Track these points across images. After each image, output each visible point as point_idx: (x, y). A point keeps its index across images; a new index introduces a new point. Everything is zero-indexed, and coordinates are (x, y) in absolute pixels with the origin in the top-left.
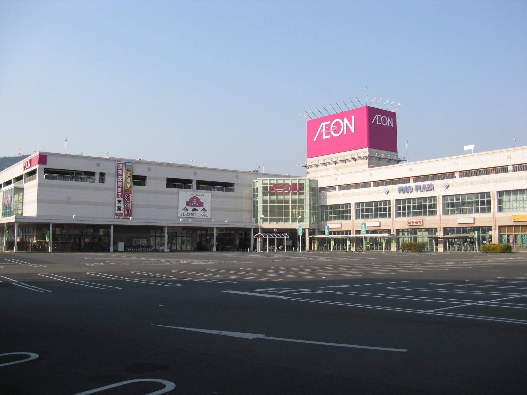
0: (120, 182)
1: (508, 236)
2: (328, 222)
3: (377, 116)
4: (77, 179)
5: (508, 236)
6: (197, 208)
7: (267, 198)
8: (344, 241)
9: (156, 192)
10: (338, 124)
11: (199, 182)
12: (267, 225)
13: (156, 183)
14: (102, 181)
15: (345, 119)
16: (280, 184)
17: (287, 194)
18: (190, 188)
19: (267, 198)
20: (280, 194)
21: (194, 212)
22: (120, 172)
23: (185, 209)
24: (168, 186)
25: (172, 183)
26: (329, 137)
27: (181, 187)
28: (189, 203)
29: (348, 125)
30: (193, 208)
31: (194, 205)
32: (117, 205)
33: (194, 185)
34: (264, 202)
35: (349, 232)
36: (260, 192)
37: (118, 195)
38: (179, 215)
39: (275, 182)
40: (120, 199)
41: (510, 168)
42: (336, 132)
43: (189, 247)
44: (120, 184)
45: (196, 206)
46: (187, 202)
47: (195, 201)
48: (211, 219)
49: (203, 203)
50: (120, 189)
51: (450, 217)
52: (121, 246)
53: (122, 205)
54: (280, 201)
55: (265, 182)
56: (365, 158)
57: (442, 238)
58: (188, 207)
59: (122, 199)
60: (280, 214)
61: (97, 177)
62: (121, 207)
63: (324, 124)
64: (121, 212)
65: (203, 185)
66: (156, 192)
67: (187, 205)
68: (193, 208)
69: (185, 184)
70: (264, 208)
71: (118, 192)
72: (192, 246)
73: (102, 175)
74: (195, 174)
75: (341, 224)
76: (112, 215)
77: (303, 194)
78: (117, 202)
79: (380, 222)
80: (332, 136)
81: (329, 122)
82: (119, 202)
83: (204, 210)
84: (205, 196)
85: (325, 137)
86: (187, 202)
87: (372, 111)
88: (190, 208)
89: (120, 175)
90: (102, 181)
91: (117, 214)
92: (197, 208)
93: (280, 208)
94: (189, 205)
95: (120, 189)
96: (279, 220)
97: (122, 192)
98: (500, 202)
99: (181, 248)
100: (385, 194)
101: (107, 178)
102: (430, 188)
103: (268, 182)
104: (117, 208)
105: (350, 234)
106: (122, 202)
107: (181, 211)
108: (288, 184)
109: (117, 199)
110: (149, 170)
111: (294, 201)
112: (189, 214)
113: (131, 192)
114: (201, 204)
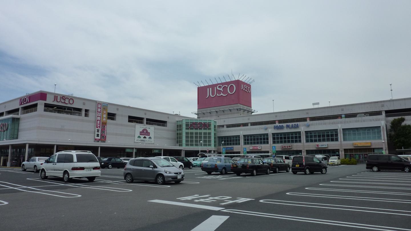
0: (99, 116)
4: (67, 113)
9: (122, 125)
11: (147, 120)
13: (122, 119)
14: (86, 115)
18: (142, 123)
19: (190, 131)
22: (99, 110)
23: (139, 137)
24: (129, 121)
25: (132, 119)
28: (142, 133)
30: (144, 136)
32: (96, 133)
34: (187, 133)
36: (184, 126)
37: (97, 126)
38: (136, 141)
40: (99, 129)
41: (343, 116)
44: (99, 118)
46: (140, 132)
47: (145, 132)
48: (154, 143)
49: (149, 133)
50: (99, 122)
53: (100, 133)
54: (196, 133)
58: (141, 136)
59: (100, 129)
61: (83, 113)
62: (99, 134)
64: (99, 138)
65: (150, 122)
66: (122, 125)
67: (140, 134)
68: (144, 136)
70: (187, 137)
71: (97, 124)
73: (87, 111)
76: (93, 140)
77: (210, 129)
82: (98, 131)
83: (150, 138)
84: (151, 129)
86: (140, 132)
88: (142, 136)
89: (99, 112)
90: (86, 115)
91: (96, 139)
95: (99, 122)
97: (100, 124)
101: (91, 114)
104: (96, 135)
106: (100, 131)
107: (136, 138)
108: (201, 123)
109: (96, 129)
111: (205, 133)
113: (106, 124)
114: (148, 134)
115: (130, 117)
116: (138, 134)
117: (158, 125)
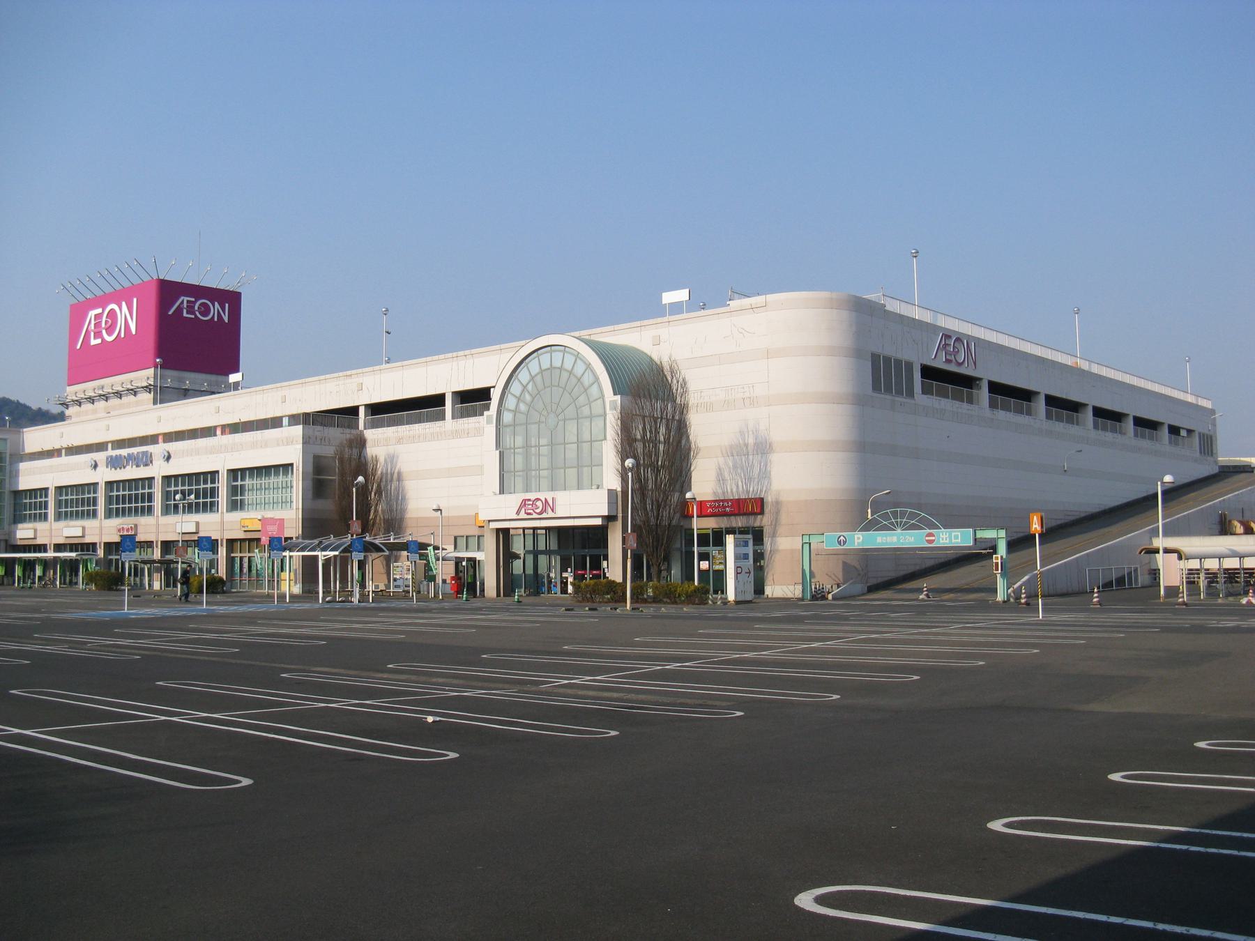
1: (241, 558)
2: (20, 526)
5: (241, 558)
8: (29, 565)
10: (112, 314)
26: (99, 341)
29: (127, 317)
35: (42, 548)
41: (285, 421)
42: (110, 330)
51: (171, 519)
56: (147, 388)
57: (159, 562)
63: (92, 313)
75: (35, 531)
79: (84, 528)
80: (103, 340)
81: (100, 311)
85: (94, 342)
87: (168, 291)
98: (234, 491)
102: (147, 460)
105: (45, 551)
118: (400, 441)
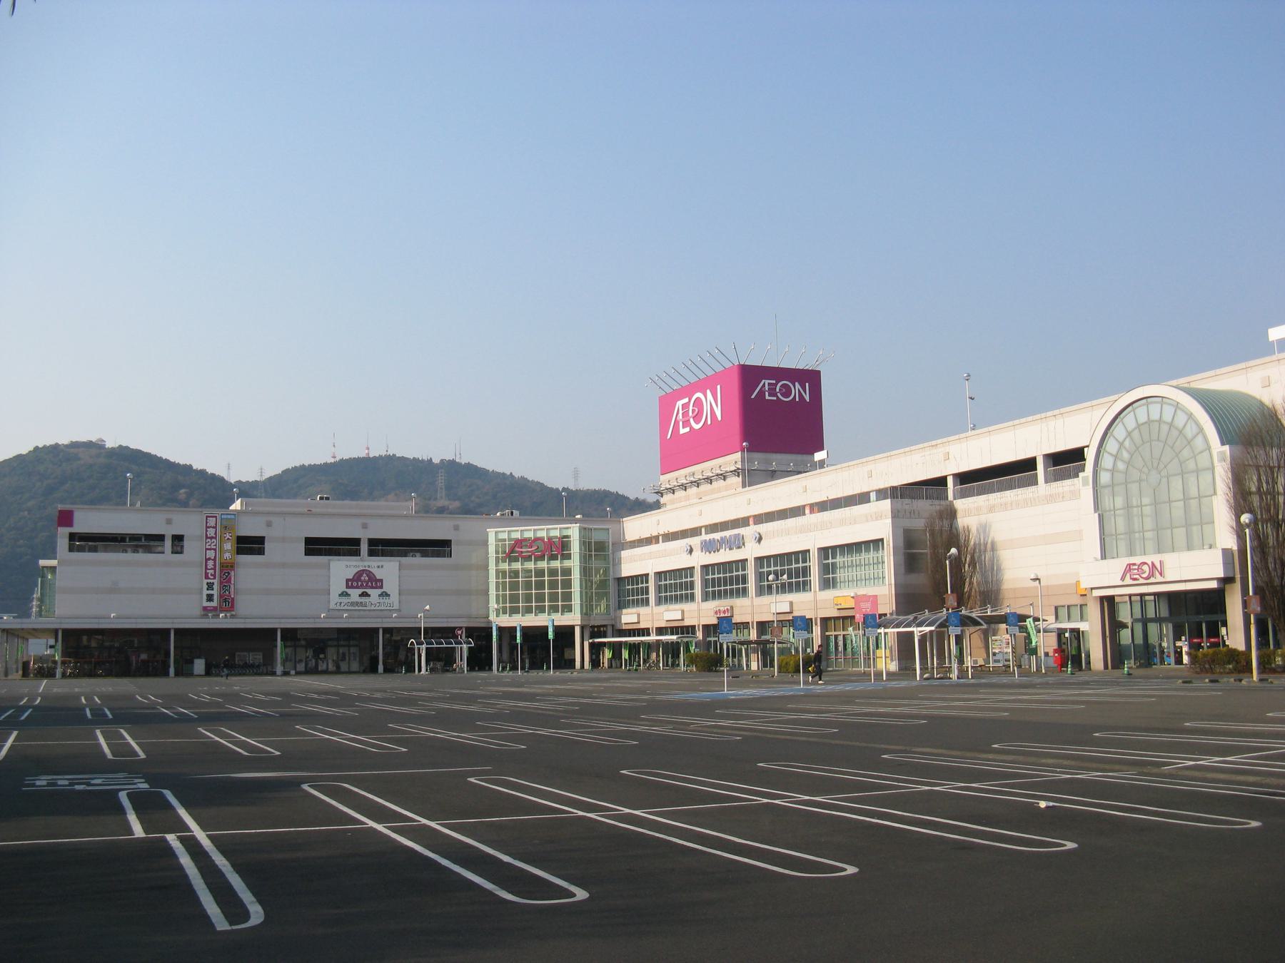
1: (836, 637)
2: (624, 611)
3: (766, 382)
4: (135, 550)
5: (836, 637)
6: (369, 591)
7: (505, 566)
8: (634, 648)
11: (373, 542)
12: (506, 621)
13: (285, 547)
15: (708, 392)
16: (526, 540)
17: (541, 558)
19: (505, 566)
20: (528, 558)
21: (364, 600)
22: (211, 532)
24: (309, 552)
25: (316, 546)
26: (687, 430)
27: (337, 553)
28: (351, 583)
29: (713, 405)
30: (360, 591)
31: (362, 587)
32: (206, 592)
33: (364, 547)
35: (645, 632)
39: (517, 535)
41: (873, 496)
42: (697, 418)
43: (355, 666)
44: (211, 554)
45: (367, 587)
46: (348, 581)
47: (365, 577)
50: (210, 563)
51: (766, 599)
52: (199, 665)
53: (215, 592)
55: (502, 536)
56: (736, 472)
57: (756, 642)
58: (349, 591)
59: (216, 582)
60: (528, 598)
61: (168, 543)
63: (680, 403)
64: (214, 604)
66: (283, 565)
67: (348, 587)
68: (360, 591)
69: (347, 547)
72: (361, 663)
73: (178, 539)
74: (365, 526)
76: (198, 611)
77: (569, 557)
78: (205, 587)
79: (683, 612)
80: (691, 428)
81: (686, 400)
82: (210, 586)
84: (387, 569)
85: (683, 431)
86: (348, 581)
87: (750, 375)
88: (355, 594)
91: (205, 608)
92: (369, 591)
93: (528, 585)
94: (352, 587)
95: (210, 563)
96: (528, 610)
97: (214, 569)
98: (826, 569)
99: (338, 667)
100: (685, 556)
102: (739, 543)
103: (505, 536)
104: (205, 597)
105: (649, 635)
106: (215, 587)
107: (334, 598)
108: (541, 539)
110: (269, 524)
112: (352, 604)
114: (378, 583)
115: (309, 541)
116: (338, 585)
117: (425, 555)
118: (991, 509)
